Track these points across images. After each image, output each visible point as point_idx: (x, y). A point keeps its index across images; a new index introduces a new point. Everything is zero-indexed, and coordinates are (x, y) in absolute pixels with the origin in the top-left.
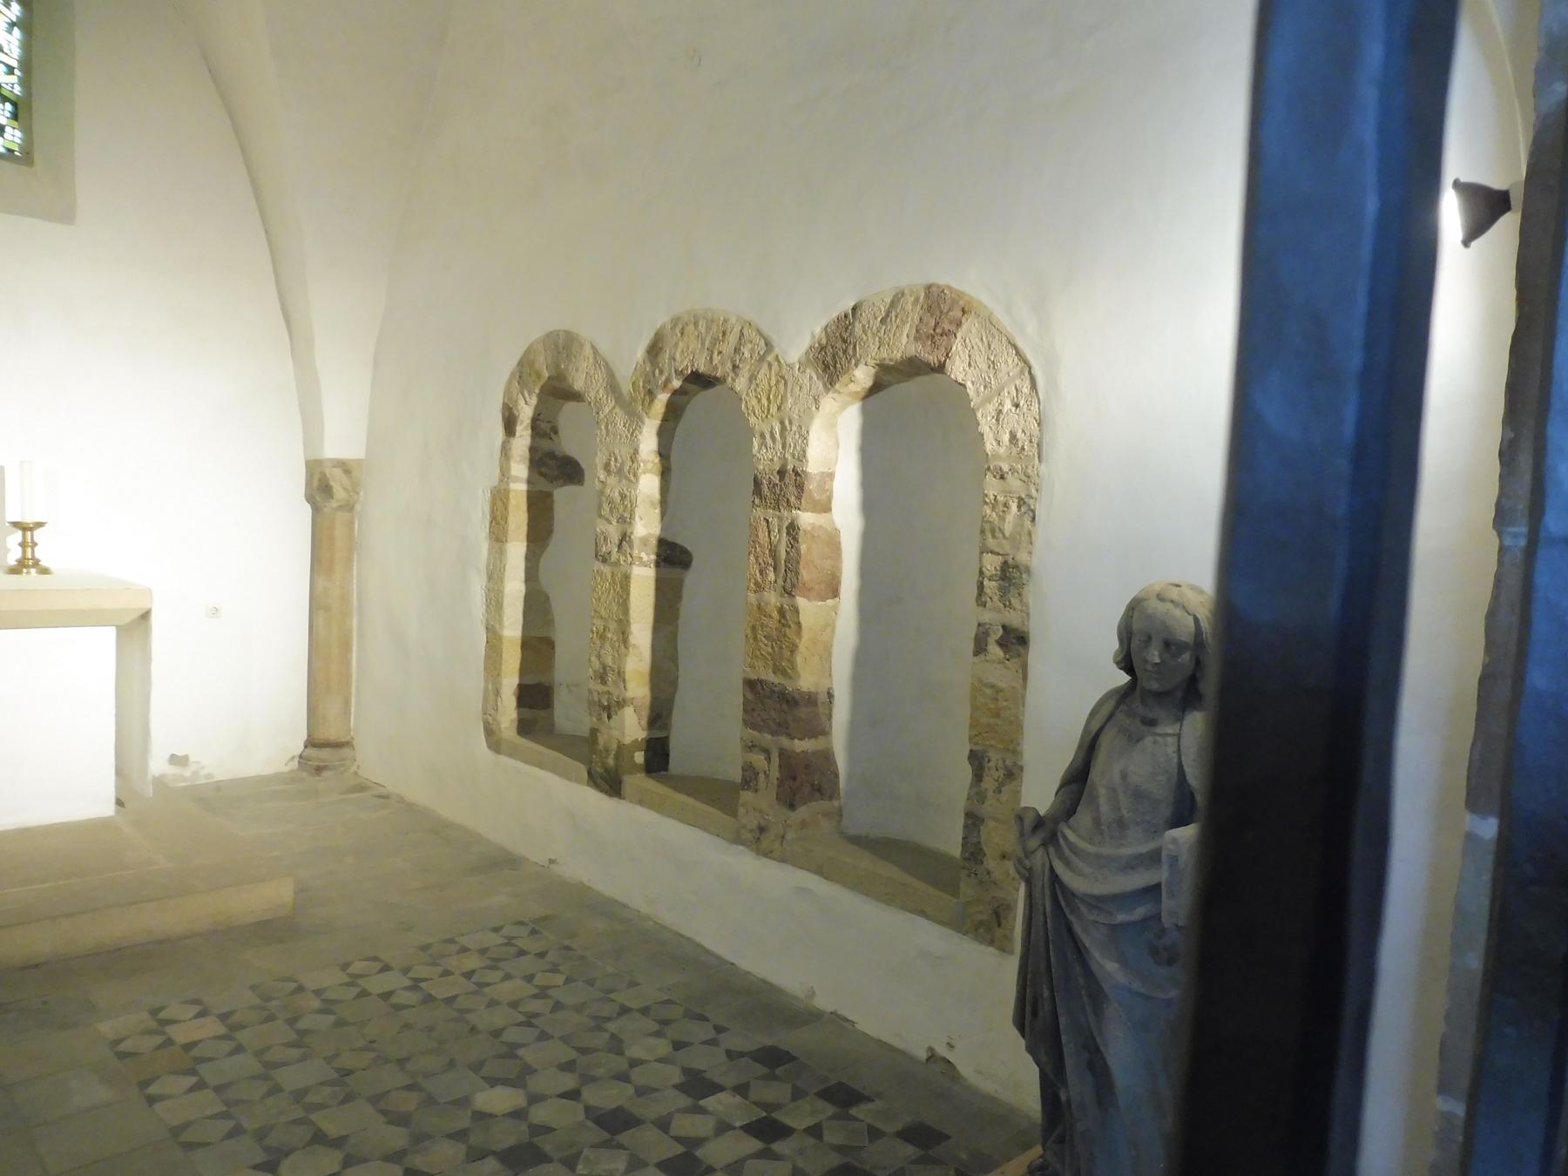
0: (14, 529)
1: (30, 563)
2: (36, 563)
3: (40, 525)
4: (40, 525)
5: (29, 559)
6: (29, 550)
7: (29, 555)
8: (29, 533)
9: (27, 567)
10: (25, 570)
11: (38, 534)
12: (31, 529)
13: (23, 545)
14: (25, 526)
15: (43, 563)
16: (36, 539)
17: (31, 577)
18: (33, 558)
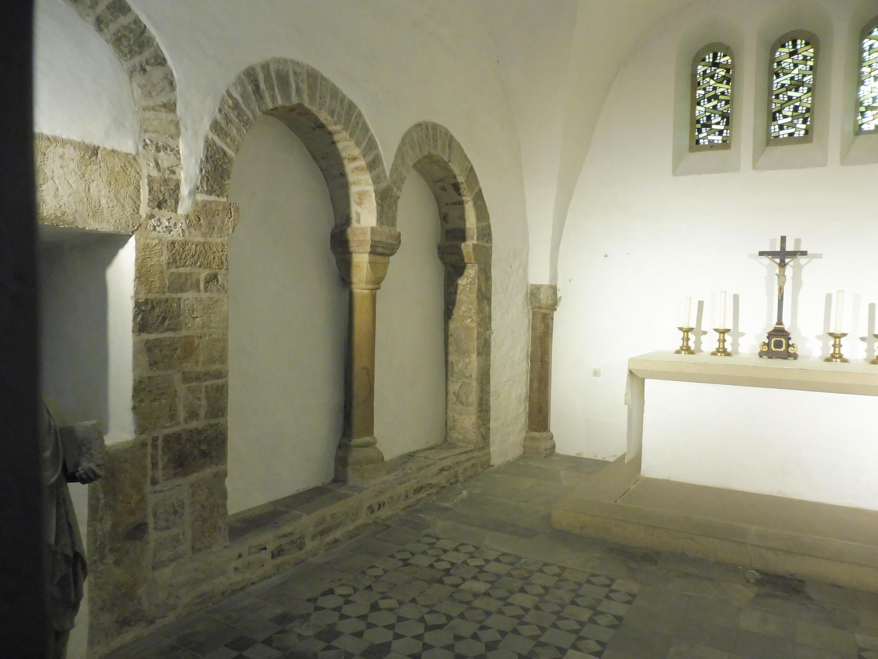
0: (876, 339)
1: (838, 356)
2: (841, 357)
3: (844, 335)
4: (844, 335)
5: (837, 354)
6: (837, 349)
7: (837, 351)
8: (838, 340)
9: (836, 358)
10: (834, 360)
11: (843, 341)
12: (839, 338)
13: (834, 346)
14: (835, 335)
15: (845, 356)
16: (841, 343)
17: (836, 365)
18: (839, 353)
